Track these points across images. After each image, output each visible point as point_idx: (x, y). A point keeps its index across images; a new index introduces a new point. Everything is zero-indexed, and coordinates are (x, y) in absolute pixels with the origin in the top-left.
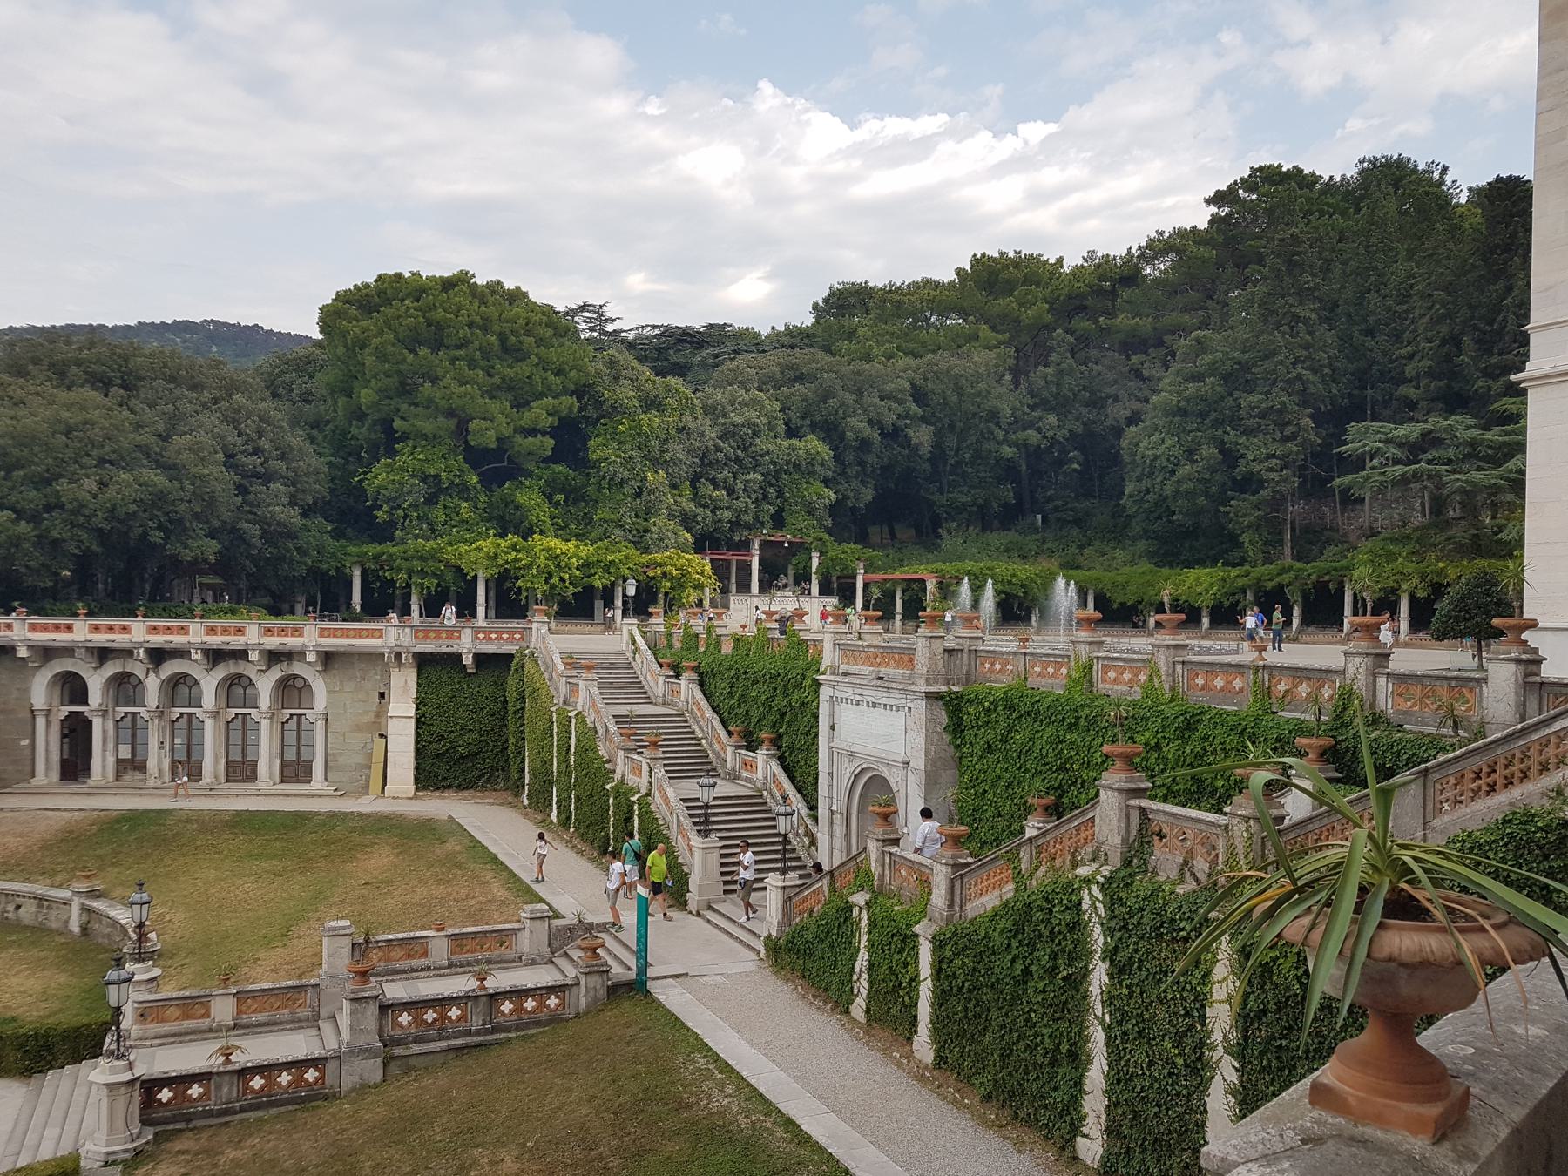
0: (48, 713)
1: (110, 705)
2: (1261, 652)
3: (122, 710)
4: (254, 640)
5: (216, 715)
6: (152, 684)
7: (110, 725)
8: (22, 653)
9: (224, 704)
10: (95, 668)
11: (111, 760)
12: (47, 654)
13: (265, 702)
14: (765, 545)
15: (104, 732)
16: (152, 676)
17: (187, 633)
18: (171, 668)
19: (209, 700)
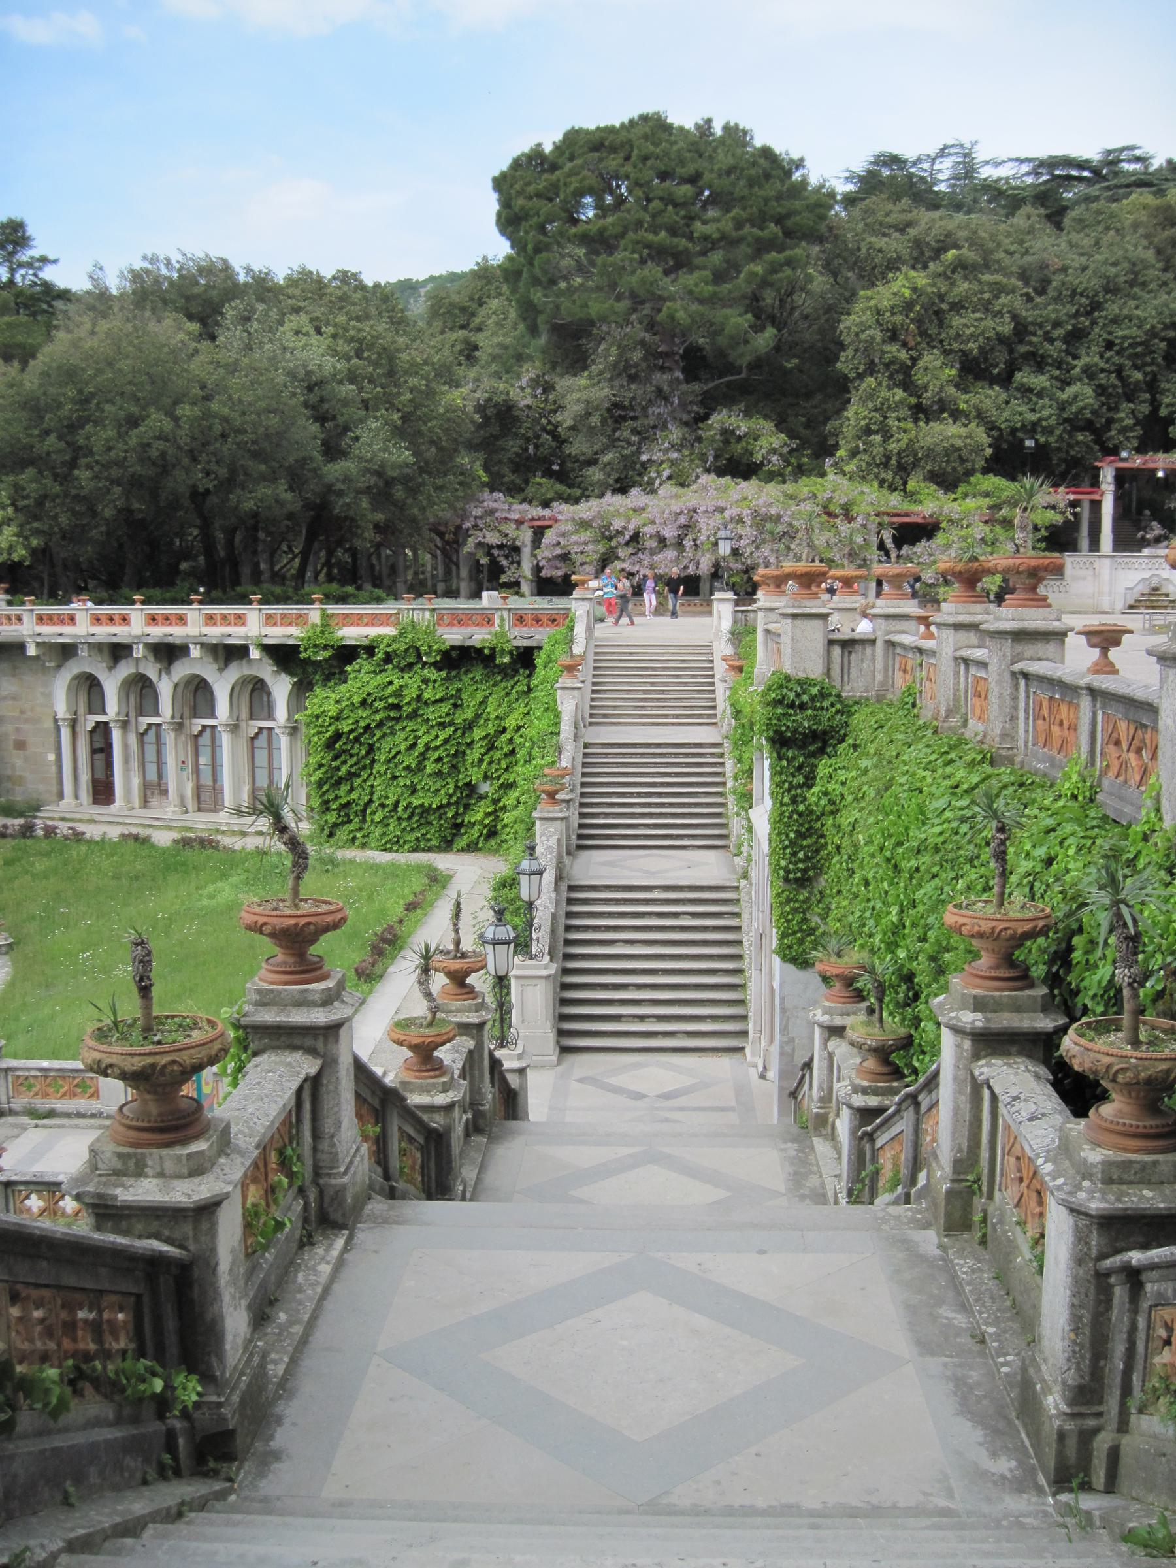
0: (73, 724)
1: (132, 714)
2: (1105, 651)
3: (145, 721)
5: (235, 728)
6: (165, 688)
7: (133, 739)
8: (32, 651)
9: (244, 714)
10: (111, 669)
11: (136, 782)
12: (66, 651)
14: (1121, 478)
15: (126, 746)
16: (164, 676)
17: (185, 624)
18: (181, 670)
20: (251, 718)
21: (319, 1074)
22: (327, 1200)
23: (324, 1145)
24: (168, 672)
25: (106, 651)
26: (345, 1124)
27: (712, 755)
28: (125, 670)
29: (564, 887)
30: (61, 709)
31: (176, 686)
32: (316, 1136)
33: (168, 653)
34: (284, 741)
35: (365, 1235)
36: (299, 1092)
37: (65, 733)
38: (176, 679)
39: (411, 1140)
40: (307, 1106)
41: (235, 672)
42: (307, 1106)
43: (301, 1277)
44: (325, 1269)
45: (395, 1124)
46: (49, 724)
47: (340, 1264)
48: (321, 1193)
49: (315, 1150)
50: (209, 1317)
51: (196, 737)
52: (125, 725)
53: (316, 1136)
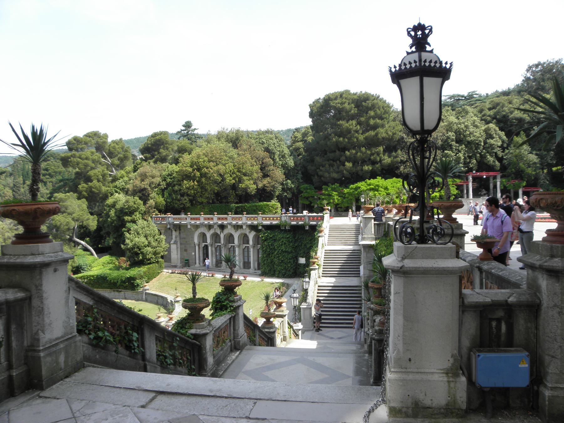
0: (199, 246)
1: (214, 243)
4: (244, 222)
5: (239, 246)
6: (222, 236)
7: (214, 249)
8: (189, 227)
9: (242, 243)
12: (197, 227)
13: (251, 242)
15: (212, 251)
16: (222, 233)
18: (226, 231)
19: (236, 241)
20: (244, 244)
21: (235, 316)
22: (236, 343)
23: (236, 332)
24: (223, 232)
25: (207, 227)
26: (240, 328)
27: (357, 253)
28: (212, 231)
29: (317, 286)
30: (196, 241)
31: (225, 236)
32: (234, 329)
33: (222, 227)
34: (251, 250)
35: (244, 352)
36: (230, 319)
37: (197, 247)
38: (225, 233)
39: (263, 339)
40: (232, 323)
41: (240, 232)
42: (232, 323)
43: (228, 358)
44: (234, 357)
45: (257, 333)
46: (193, 245)
47: (237, 357)
48: (235, 342)
49: (234, 333)
50: (204, 357)
51: (230, 249)
52: (212, 245)
53: (234, 329)
